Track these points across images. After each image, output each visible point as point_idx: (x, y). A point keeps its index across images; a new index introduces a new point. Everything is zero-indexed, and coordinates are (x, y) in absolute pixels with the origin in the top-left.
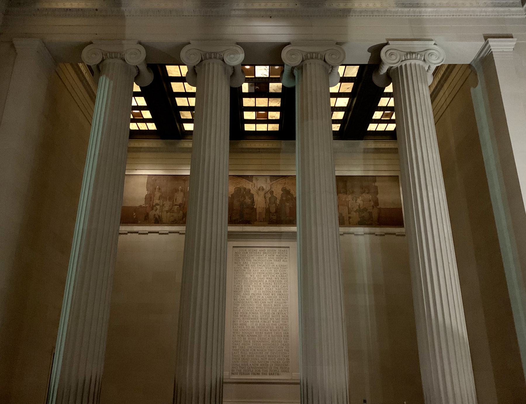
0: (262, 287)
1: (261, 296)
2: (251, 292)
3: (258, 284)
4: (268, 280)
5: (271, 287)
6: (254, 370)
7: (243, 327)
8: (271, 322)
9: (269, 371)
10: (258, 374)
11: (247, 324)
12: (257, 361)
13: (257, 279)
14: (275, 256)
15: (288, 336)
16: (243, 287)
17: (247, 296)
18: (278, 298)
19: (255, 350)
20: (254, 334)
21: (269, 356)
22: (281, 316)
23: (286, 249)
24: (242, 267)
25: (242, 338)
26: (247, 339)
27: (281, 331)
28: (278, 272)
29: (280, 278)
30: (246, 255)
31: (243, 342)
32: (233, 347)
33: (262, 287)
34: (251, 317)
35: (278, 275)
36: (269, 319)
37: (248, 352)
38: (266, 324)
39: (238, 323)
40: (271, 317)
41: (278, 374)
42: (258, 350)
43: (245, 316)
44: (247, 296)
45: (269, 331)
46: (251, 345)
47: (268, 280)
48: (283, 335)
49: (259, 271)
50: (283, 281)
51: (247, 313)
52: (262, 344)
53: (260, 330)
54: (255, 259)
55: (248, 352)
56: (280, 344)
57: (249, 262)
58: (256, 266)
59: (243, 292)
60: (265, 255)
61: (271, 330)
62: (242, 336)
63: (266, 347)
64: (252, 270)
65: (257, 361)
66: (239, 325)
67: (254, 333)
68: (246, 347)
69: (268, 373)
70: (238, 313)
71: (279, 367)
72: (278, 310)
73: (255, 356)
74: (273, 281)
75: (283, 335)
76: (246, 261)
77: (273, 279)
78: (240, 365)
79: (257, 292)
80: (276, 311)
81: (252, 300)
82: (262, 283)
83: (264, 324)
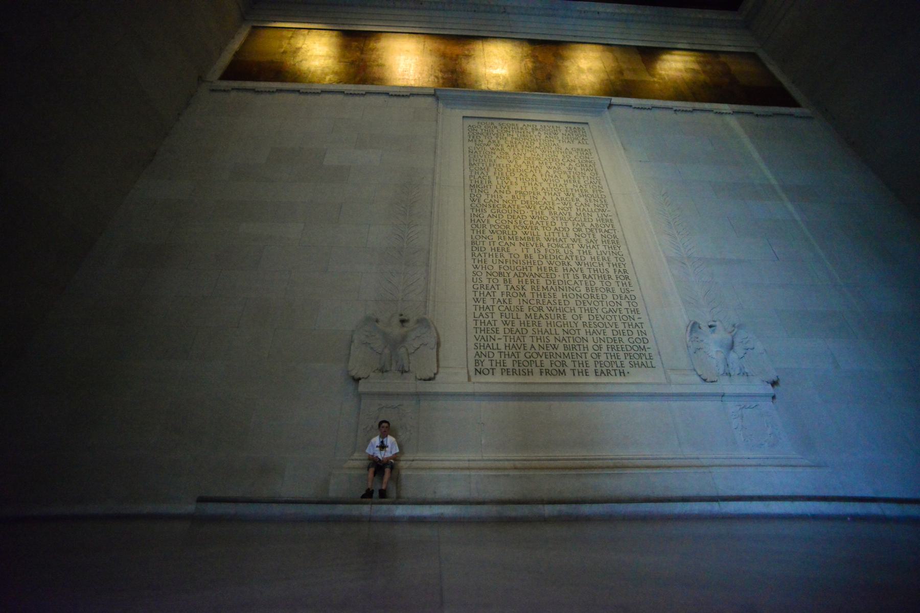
0: (540, 180)
1: (540, 198)
2: (513, 189)
3: (530, 175)
4: (551, 171)
5: (562, 182)
6: (547, 363)
7: (502, 256)
8: (576, 246)
9: (591, 362)
10: (563, 373)
11: (512, 248)
12: (552, 338)
13: (524, 167)
14: (560, 136)
15: (627, 278)
16: (493, 179)
17: (504, 195)
18: (582, 200)
19: (540, 309)
20: (534, 270)
21: (584, 324)
22: (598, 235)
23: (581, 126)
24: (488, 148)
25: (501, 279)
26: (515, 282)
27: (606, 266)
28: (573, 158)
29: (579, 169)
30: (495, 131)
31: (503, 288)
32: (477, 300)
33: (540, 180)
34: (520, 234)
35: (573, 164)
36: (569, 241)
37: (522, 316)
38: (561, 250)
39: (487, 245)
40: (572, 234)
41: (622, 373)
42: (550, 309)
43: (504, 232)
44: (504, 195)
45: (574, 265)
46: (529, 296)
47: (551, 171)
48: (612, 273)
49: (528, 155)
50: (588, 174)
51: (507, 227)
52: (559, 295)
53: (550, 263)
54: (515, 136)
55: (522, 316)
56: (610, 295)
57: (502, 142)
58: (520, 147)
59: (494, 188)
60: (536, 133)
61: (579, 264)
62: (500, 274)
63: (572, 301)
64: (511, 153)
65: (552, 338)
66: (488, 250)
67: (534, 270)
68: (515, 302)
69: (591, 370)
70: (484, 226)
71: (621, 354)
72: (588, 225)
73: (544, 327)
74: (565, 172)
75: (612, 273)
76: (494, 138)
77: (563, 168)
78: (502, 347)
79: (529, 189)
80: (583, 225)
81: (519, 203)
82: (538, 175)
83: (558, 251)
